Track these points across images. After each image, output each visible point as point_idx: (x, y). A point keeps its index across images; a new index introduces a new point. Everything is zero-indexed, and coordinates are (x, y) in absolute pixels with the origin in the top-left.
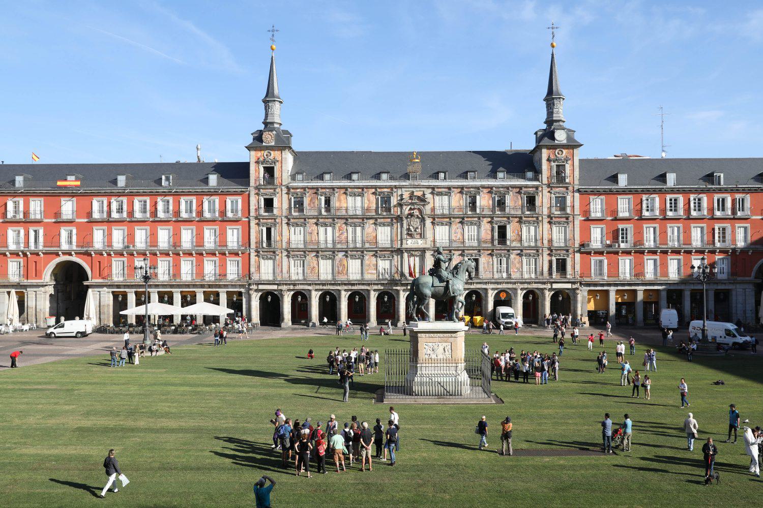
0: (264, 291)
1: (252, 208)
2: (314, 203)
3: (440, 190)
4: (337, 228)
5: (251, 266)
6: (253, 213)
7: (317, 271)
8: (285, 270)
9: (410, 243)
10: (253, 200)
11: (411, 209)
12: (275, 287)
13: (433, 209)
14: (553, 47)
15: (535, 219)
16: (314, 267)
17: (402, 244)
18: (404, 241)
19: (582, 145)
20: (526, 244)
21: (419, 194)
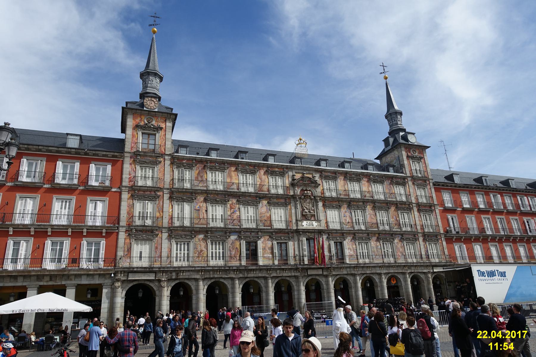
0: (135, 283)
1: (126, 176)
2: (202, 177)
3: (326, 174)
4: (229, 206)
5: (119, 249)
6: (126, 183)
7: (205, 255)
8: (165, 254)
9: (305, 225)
10: (127, 167)
11: (302, 190)
12: (152, 277)
13: (323, 193)
14: (386, 78)
15: (407, 206)
16: (201, 251)
17: (297, 226)
18: (299, 223)
19: (429, 147)
20: (404, 229)
21: (310, 176)
